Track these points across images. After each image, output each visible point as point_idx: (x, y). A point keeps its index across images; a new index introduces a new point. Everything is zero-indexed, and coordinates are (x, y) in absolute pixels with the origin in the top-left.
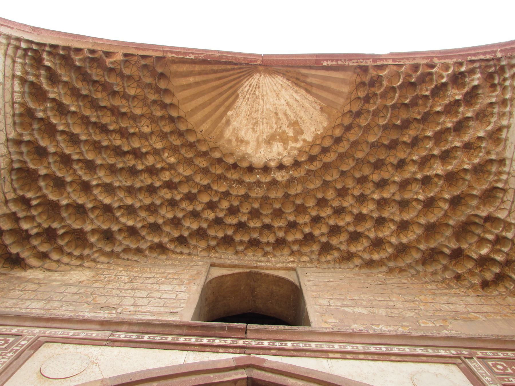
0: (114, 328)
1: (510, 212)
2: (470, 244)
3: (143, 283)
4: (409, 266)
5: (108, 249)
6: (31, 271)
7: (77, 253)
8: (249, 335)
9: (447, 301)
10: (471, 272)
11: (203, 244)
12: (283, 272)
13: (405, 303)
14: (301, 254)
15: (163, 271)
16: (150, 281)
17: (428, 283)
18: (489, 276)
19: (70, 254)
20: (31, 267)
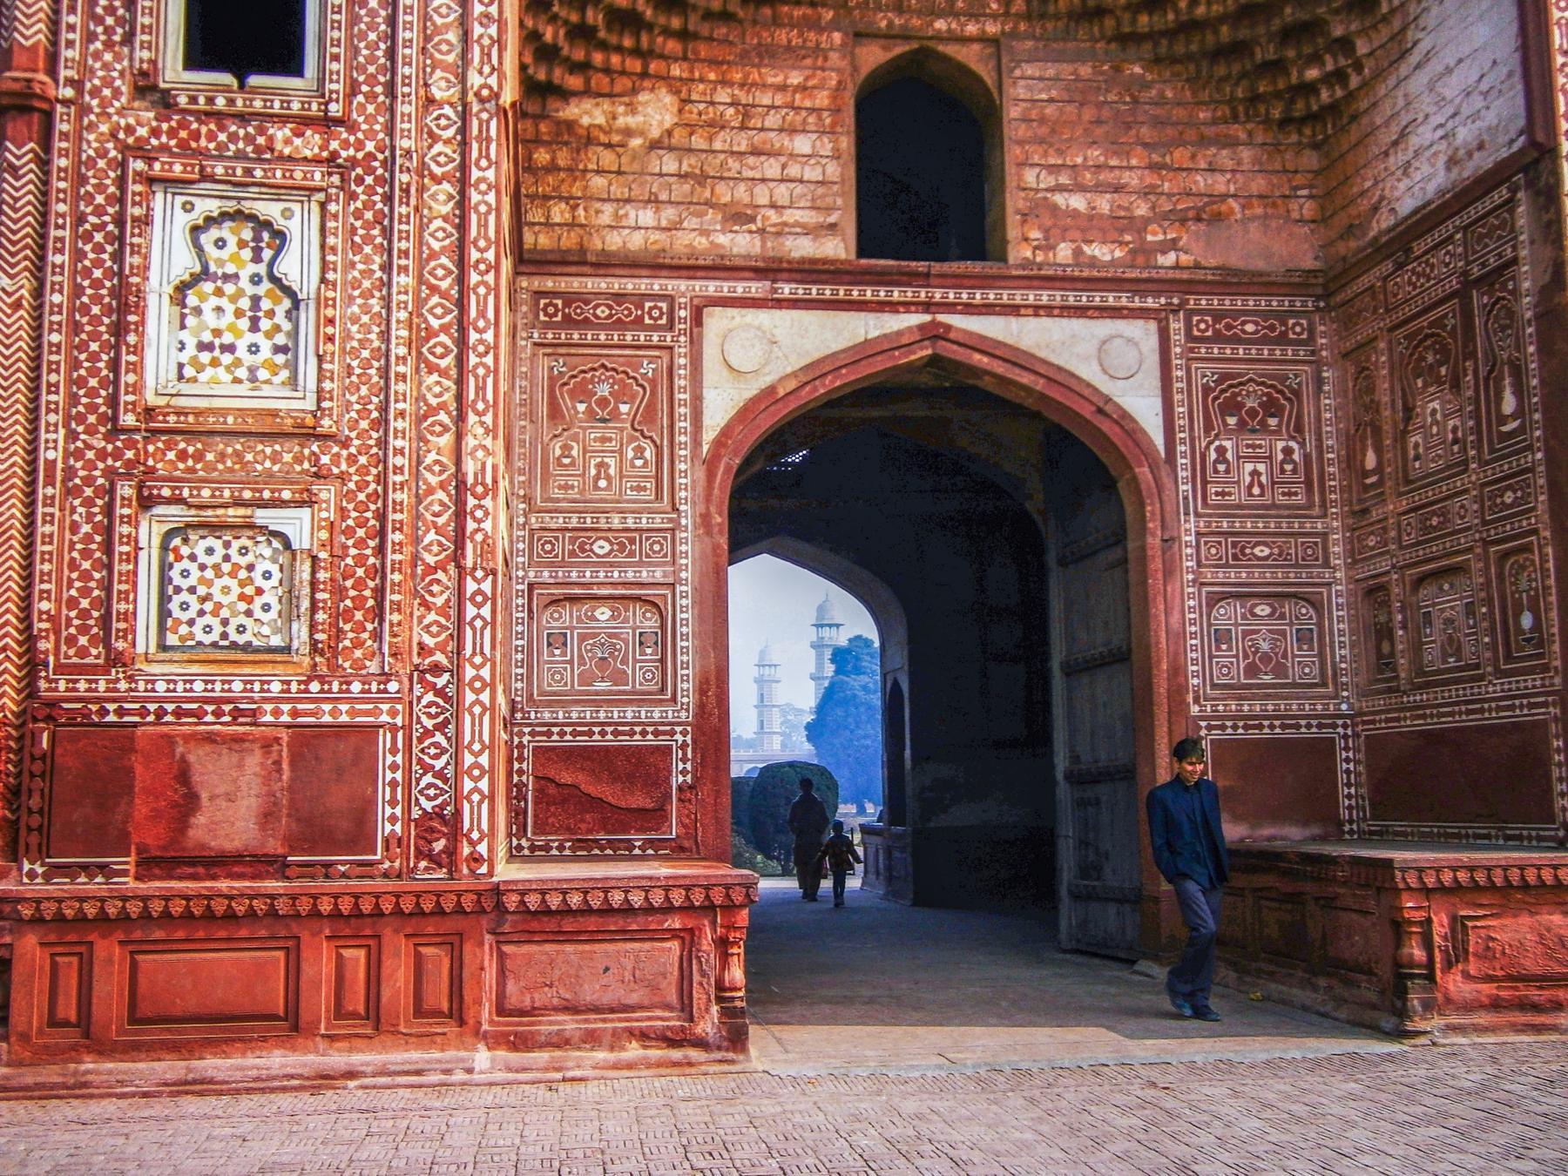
0: (771, 276)
1: (1371, 54)
2: (1299, 56)
3: (762, 129)
4: (1189, 57)
5: (676, 23)
6: (573, 101)
7: (628, 42)
8: (933, 281)
9: (1210, 163)
10: (1278, 95)
12: (976, 47)
13: (1146, 172)
15: (779, 79)
16: (773, 120)
17: (1202, 103)
18: (1299, 108)
19: (619, 49)
20: (574, 94)
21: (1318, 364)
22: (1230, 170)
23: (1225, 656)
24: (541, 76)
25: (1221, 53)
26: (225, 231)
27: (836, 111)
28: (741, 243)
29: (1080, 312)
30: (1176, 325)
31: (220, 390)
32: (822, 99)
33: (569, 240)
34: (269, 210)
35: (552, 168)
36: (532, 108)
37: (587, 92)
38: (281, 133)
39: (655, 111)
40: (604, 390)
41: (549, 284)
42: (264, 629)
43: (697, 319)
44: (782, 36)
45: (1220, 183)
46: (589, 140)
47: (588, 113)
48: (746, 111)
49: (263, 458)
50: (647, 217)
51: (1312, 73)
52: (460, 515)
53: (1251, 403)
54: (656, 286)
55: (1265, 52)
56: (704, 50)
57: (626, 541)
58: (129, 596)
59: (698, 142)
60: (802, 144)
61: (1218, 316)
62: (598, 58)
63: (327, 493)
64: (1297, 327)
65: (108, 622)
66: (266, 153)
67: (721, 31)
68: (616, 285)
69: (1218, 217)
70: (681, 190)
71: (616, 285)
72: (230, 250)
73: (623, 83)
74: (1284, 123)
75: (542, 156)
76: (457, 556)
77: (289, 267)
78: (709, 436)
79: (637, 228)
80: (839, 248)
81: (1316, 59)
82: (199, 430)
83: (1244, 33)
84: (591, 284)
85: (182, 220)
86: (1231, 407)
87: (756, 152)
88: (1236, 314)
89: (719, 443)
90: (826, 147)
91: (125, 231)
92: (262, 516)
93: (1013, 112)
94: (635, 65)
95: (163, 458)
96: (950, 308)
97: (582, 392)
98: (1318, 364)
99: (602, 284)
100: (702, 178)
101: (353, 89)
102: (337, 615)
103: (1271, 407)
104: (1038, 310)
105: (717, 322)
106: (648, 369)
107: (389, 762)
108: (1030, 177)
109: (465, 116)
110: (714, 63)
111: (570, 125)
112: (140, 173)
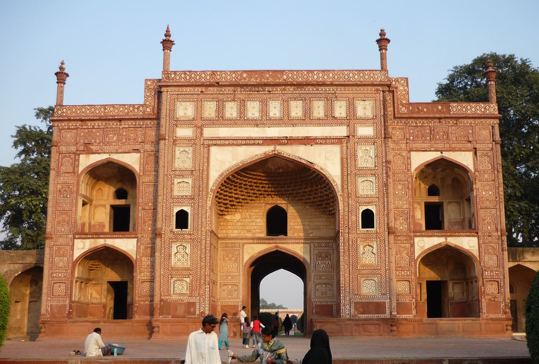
11: (263, 196)
14: (289, 197)
21: (333, 250)
22: (321, 221)
23: (317, 293)
24: (222, 213)
25: (318, 205)
26: (180, 247)
27: (263, 215)
28: (249, 235)
29: (298, 243)
30: (312, 245)
31: (179, 265)
32: (261, 214)
33: (226, 235)
34: (185, 245)
35: (223, 225)
36: (221, 217)
37: (228, 215)
38: (186, 236)
39: (237, 216)
40: (230, 256)
41: (223, 242)
42: (184, 292)
43: (243, 246)
44: (256, 205)
45: (320, 224)
46: (229, 221)
47: (228, 217)
48: (250, 216)
49: (185, 272)
50: (236, 232)
51: (331, 209)
52: (205, 278)
53: (323, 256)
54: (238, 241)
55: (324, 206)
56: (244, 207)
57: (233, 277)
58: (170, 288)
59: (244, 221)
60: (258, 220)
61: (318, 243)
62: (229, 210)
63: (191, 276)
64: (331, 245)
65: (169, 290)
66: (184, 238)
67: (247, 205)
68: (232, 241)
69: (319, 228)
70: (241, 228)
71: (232, 241)
72: (181, 249)
73: (233, 213)
74: (329, 214)
75: (222, 224)
76: (205, 283)
77: (187, 251)
78: (245, 262)
79: (234, 233)
80: (263, 235)
81: (330, 207)
82: (177, 269)
83: (321, 203)
84: (228, 241)
85: (176, 246)
86: (320, 256)
87: (252, 222)
88: (321, 243)
89: (246, 263)
90: (262, 220)
91: (170, 247)
92: (184, 279)
93: (289, 214)
94: (235, 210)
95: (174, 273)
96: (279, 243)
97: (227, 257)
98: (333, 250)
99: (230, 241)
100: (244, 226)
101: (194, 230)
102: (192, 290)
103: (326, 256)
104: (292, 243)
105: (246, 246)
106: (236, 253)
107: (197, 306)
108: (291, 224)
109: (206, 232)
110: (246, 209)
111: (226, 219)
112: (172, 241)
